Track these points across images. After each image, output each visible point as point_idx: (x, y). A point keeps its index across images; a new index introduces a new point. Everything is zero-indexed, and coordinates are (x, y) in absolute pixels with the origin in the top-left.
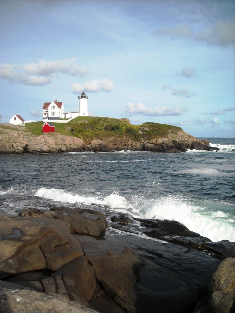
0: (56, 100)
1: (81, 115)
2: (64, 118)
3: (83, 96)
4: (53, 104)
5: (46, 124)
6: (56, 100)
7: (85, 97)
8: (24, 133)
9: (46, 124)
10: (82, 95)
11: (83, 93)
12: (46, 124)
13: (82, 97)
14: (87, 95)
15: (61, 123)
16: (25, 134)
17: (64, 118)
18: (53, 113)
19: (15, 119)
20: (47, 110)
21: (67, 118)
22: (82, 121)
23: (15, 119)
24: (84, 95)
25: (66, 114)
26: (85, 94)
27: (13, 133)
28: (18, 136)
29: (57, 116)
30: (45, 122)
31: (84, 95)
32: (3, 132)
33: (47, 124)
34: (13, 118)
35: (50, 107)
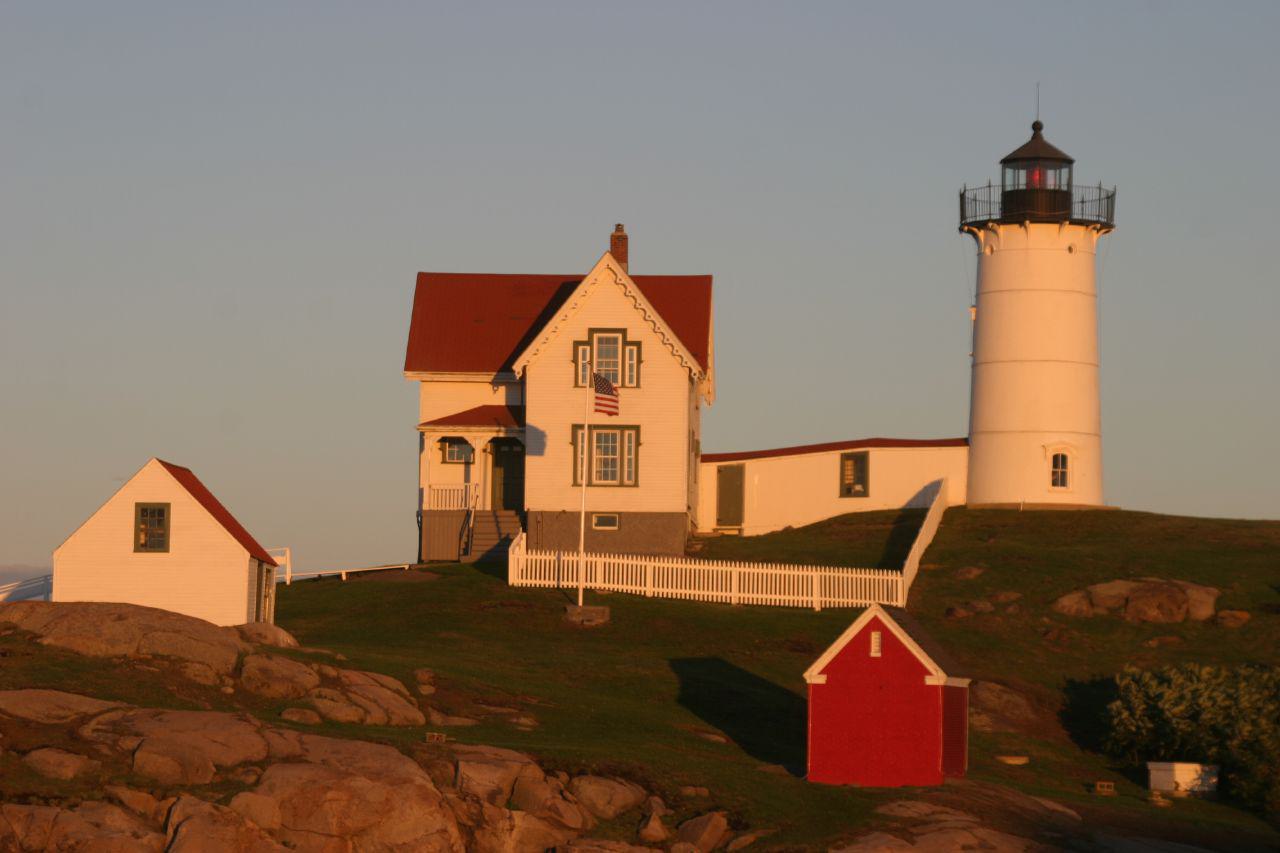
0: (619, 246)
1: (1025, 486)
2: (707, 521)
3: (1036, 189)
4: (604, 301)
5: (875, 651)
6: (619, 246)
7: (1055, 208)
8: (545, 792)
9: (863, 638)
10: (1020, 179)
11: (1036, 155)
12: (875, 651)
13: (1019, 208)
14: (1108, 187)
15: (724, 607)
16: (573, 817)
17: (707, 521)
18: (612, 450)
19: (152, 528)
20: (498, 398)
21: (758, 521)
22: (1117, 589)
23: (152, 528)
24: (1052, 179)
25: (750, 465)
26: (1068, 162)
27: (375, 792)
28: (454, 831)
29: (662, 485)
30: (859, 611)
31: (1052, 179)
32: (152, 762)
33: (888, 639)
34: (118, 520)
35: (547, 362)
